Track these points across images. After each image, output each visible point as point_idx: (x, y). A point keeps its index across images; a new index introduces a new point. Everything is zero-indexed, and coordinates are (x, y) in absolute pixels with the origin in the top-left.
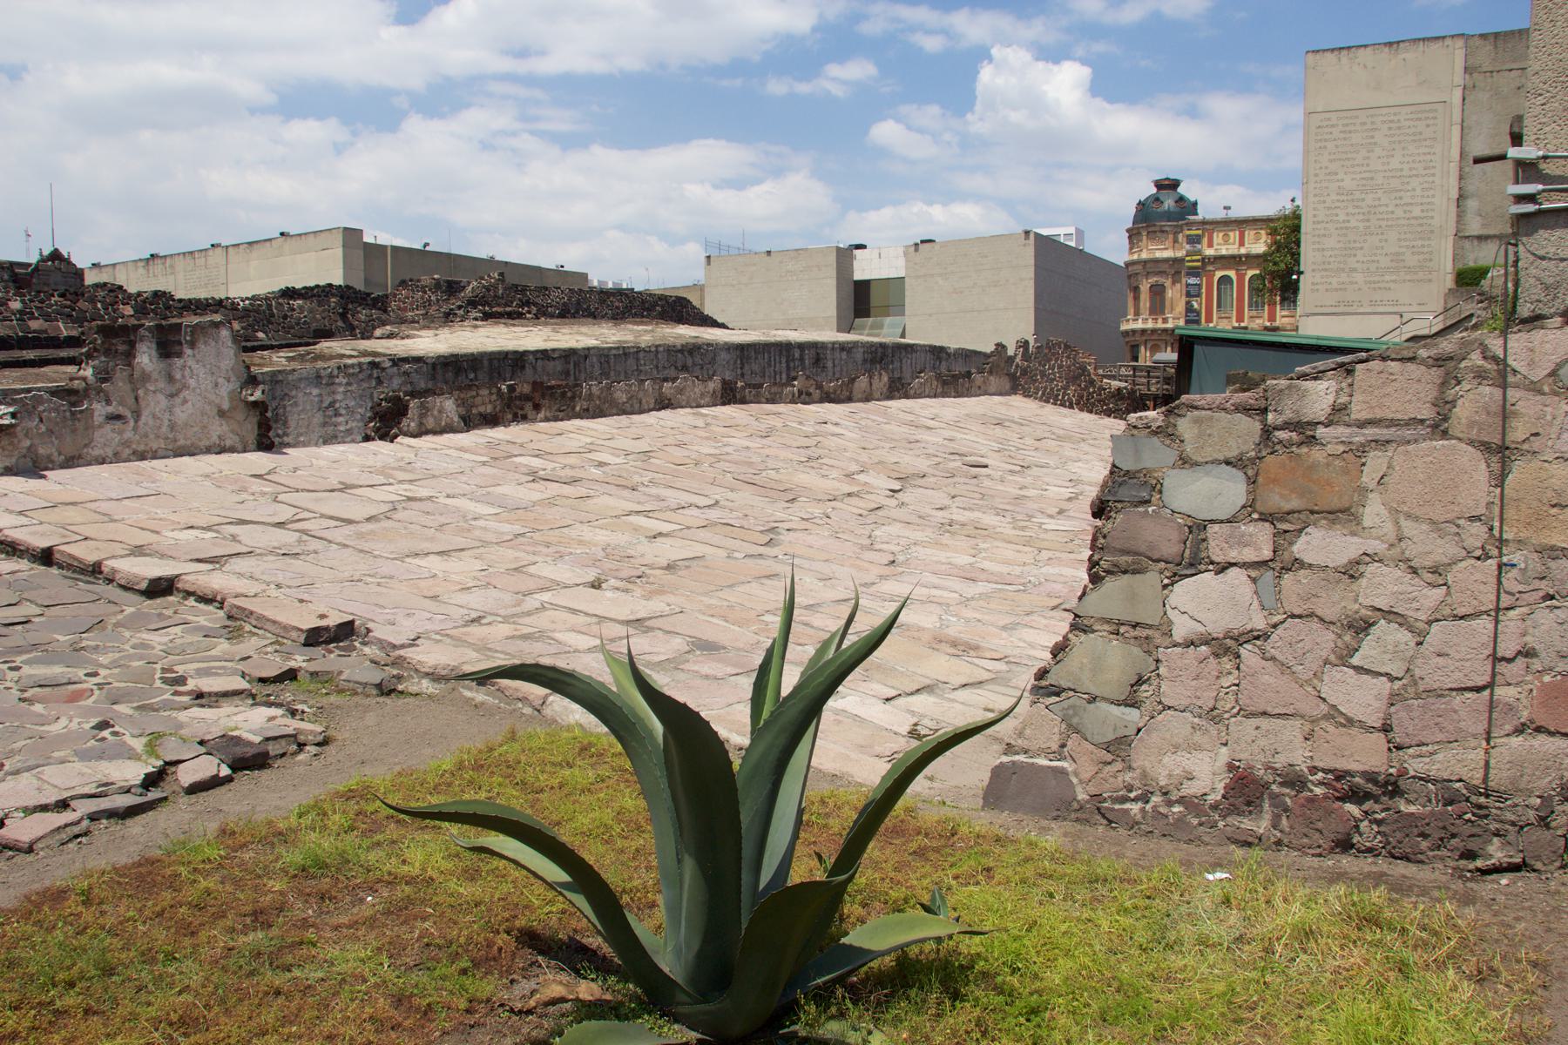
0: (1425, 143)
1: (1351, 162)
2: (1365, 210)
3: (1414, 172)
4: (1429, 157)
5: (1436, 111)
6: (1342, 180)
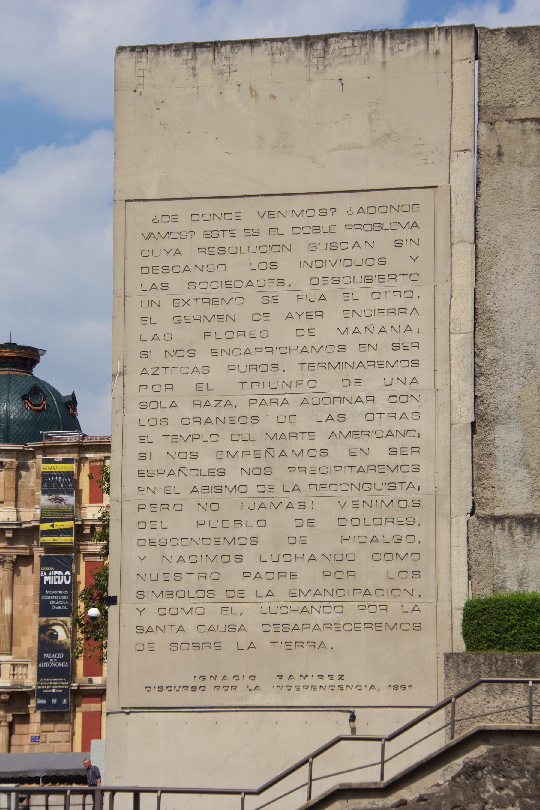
0: (392, 285)
1: (228, 326)
2: (262, 445)
3: (371, 355)
4: (401, 320)
5: (416, 208)
6: (206, 370)
